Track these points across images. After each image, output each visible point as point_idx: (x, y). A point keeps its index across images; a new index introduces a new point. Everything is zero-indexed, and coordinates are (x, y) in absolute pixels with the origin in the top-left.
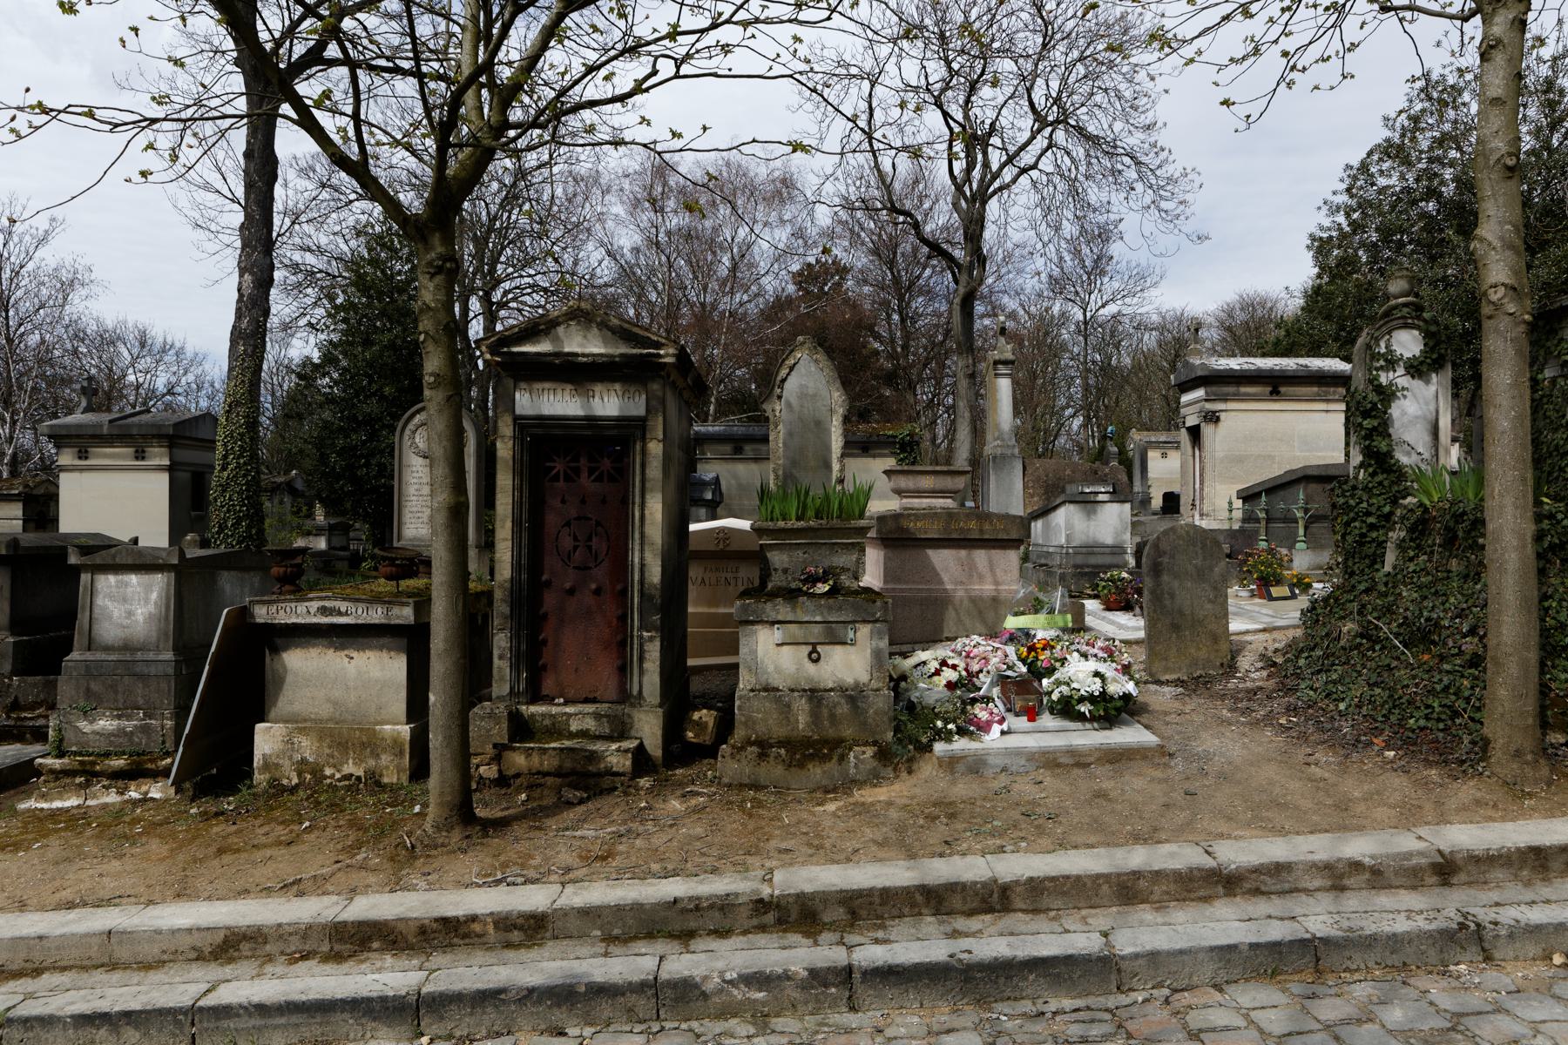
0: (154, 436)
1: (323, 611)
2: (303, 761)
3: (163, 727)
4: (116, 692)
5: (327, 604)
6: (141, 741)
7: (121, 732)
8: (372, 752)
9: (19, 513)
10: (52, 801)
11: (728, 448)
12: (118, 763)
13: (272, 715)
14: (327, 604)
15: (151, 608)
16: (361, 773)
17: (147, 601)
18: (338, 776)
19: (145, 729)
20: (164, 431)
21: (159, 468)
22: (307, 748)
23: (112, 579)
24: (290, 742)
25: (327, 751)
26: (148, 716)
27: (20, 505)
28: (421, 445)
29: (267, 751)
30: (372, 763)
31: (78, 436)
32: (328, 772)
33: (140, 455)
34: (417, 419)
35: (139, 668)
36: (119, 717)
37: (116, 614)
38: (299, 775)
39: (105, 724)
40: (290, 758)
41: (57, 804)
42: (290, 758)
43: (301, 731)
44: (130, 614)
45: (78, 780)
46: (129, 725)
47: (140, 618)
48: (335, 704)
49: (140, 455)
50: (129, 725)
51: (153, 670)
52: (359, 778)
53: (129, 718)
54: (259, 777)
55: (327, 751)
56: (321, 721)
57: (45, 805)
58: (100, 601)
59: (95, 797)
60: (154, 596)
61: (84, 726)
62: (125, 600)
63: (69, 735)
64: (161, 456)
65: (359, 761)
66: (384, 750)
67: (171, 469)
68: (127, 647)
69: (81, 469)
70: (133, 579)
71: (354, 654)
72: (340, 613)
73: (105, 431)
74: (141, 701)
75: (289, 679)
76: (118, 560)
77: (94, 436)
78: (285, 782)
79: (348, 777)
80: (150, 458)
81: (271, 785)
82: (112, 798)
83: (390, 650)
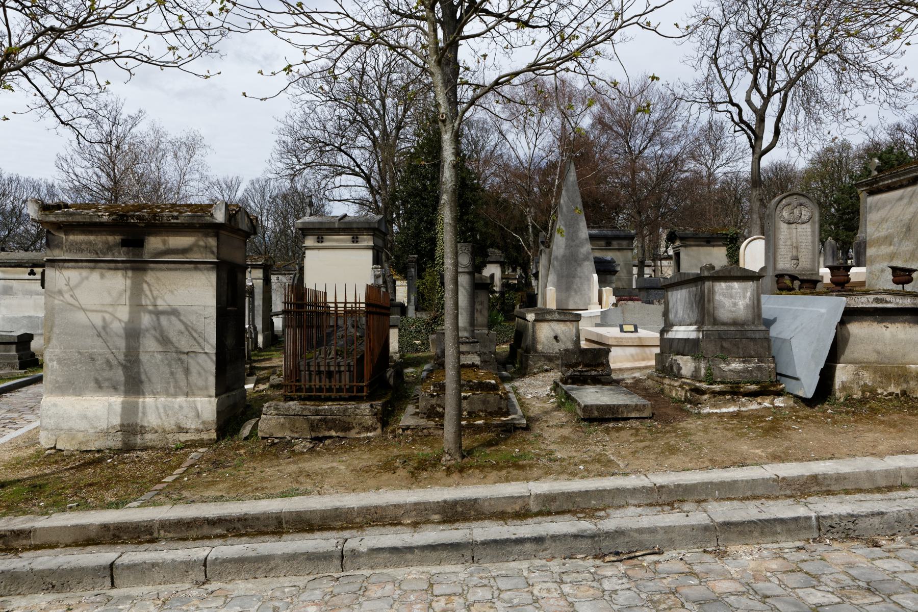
0: (365, 229)
1: (877, 300)
2: (865, 384)
3: (769, 367)
4: (738, 348)
5: (879, 296)
6: (758, 375)
7: (746, 370)
8: (904, 380)
9: (261, 276)
10: (720, 408)
11: (603, 243)
12: (753, 387)
13: (842, 359)
14: (879, 296)
15: (748, 301)
16: (899, 392)
17: (744, 297)
18: (885, 393)
19: (759, 369)
20: (372, 226)
21: (367, 248)
22: (867, 378)
23: (723, 285)
24: (857, 374)
25: (879, 379)
26: (760, 361)
27: (261, 271)
28: (786, 217)
29: (844, 380)
30: (904, 386)
31: (319, 229)
32: (879, 391)
33: (355, 240)
34: (784, 202)
35: (749, 335)
36: (744, 362)
37: (727, 304)
38: (863, 392)
39: (736, 366)
40: (858, 383)
41: (724, 410)
42: (858, 383)
43: (863, 368)
44: (735, 304)
45: (728, 397)
46: (750, 366)
47: (742, 307)
48: (878, 353)
49: (355, 240)
50: (750, 366)
51: (757, 336)
52: (897, 395)
53: (750, 362)
54: (840, 395)
55: (879, 379)
56: (870, 363)
57: (718, 411)
58: (718, 297)
59: (744, 405)
60: (749, 294)
61: (723, 366)
62: (731, 297)
63: (716, 372)
64: (368, 240)
65: (897, 384)
66: (912, 379)
67: (373, 248)
68: (735, 323)
69: (319, 248)
70: (736, 285)
71: (889, 325)
72: (887, 302)
73: (336, 226)
74: (753, 353)
75: (851, 339)
76: (732, 274)
77: (328, 229)
78: (855, 397)
79: (891, 394)
80: (361, 242)
81: (846, 399)
82: (754, 406)
83: (909, 323)
